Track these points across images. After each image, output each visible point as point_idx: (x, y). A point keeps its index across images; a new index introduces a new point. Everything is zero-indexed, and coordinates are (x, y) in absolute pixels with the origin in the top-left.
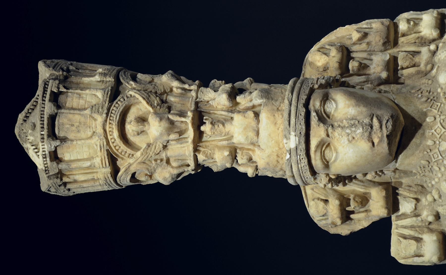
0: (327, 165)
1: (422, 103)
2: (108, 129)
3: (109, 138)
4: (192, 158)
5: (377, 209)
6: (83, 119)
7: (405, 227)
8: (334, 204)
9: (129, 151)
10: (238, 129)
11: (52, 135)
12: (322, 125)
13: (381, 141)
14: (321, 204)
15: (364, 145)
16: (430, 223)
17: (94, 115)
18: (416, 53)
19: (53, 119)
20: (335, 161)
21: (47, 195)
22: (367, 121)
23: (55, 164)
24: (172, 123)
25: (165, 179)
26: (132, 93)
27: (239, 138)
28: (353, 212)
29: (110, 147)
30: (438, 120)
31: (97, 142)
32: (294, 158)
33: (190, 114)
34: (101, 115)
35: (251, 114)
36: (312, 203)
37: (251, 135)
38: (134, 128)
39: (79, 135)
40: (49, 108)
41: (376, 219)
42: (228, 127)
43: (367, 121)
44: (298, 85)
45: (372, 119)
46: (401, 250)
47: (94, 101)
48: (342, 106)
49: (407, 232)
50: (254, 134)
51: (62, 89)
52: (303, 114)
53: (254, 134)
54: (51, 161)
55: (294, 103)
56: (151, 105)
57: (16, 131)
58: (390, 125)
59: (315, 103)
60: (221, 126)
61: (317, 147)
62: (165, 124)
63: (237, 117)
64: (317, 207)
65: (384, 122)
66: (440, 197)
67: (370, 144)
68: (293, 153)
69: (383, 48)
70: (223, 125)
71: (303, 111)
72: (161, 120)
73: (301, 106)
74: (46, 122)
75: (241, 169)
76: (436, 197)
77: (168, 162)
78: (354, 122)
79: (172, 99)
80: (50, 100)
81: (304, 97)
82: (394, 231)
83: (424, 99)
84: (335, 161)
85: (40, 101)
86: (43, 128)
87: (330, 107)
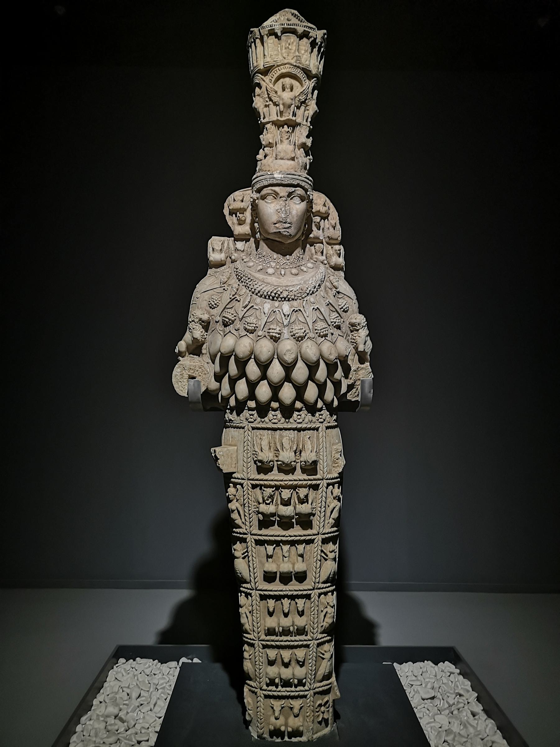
0: (263, 198)
1: (296, 254)
2: (287, 66)
3: (282, 67)
4: (268, 120)
5: (238, 230)
6: (293, 51)
7: (228, 244)
8: (242, 205)
9: (273, 80)
10: (285, 148)
11: (284, 31)
12: (287, 194)
13: (277, 228)
14: (241, 199)
15: (275, 218)
16: (230, 258)
17: (295, 58)
18: (322, 253)
19: (294, 32)
20: (266, 202)
21: (247, 31)
22: (288, 220)
23: (266, 33)
24: (289, 107)
25: (256, 103)
26: (307, 83)
27: (280, 147)
28: (236, 216)
29: (276, 67)
30: (288, 261)
31: (280, 59)
32: (268, 176)
33: (294, 118)
34: (296, 62)
35: (293, 156)
36: (241, 193)
37: (282, 155)
38: (287, 82)
39: (284, 48)
40: (300, 30)
41: (232, 228)
42: (286, 142)
43: (288, 220)
44: (310, 182)
45: (289, 223)
46: (215, 242)
47: (303, 60)
48: (297, 207)
49: (226, 245)
50: (283, 156)
51: (311, 40)
52: (294, 183)
53: (283, 156)
54: (269, 30)
55: (300, 178)
56: (299, 95)
57: (287, 10)
58: (286, 233)
59: (300, 191)
60: (287, 137)
61: (275, 191)
62: (289, 102)
63: (292, 147)
64: (239, 196)
65: (287, 230)
66: (245, 262)
67: (275, 222)
68: (271, 176)
69: (326, 236)
70: (288, 139)
71: (295, 183)
72: (292, 99)
73: (298, 182)
74: (291, 27)
75: (261, 150)
76: (245, 260)
77: (266, 106)
78: (288, 213)
79: (303, 108)
80: (304, 30)
81: (303, 184)
82: (226, 238)
83: (298, 255)
84: (266, 202)
85: (304, 24)
86: (289, 25)
87: (297, 200)
